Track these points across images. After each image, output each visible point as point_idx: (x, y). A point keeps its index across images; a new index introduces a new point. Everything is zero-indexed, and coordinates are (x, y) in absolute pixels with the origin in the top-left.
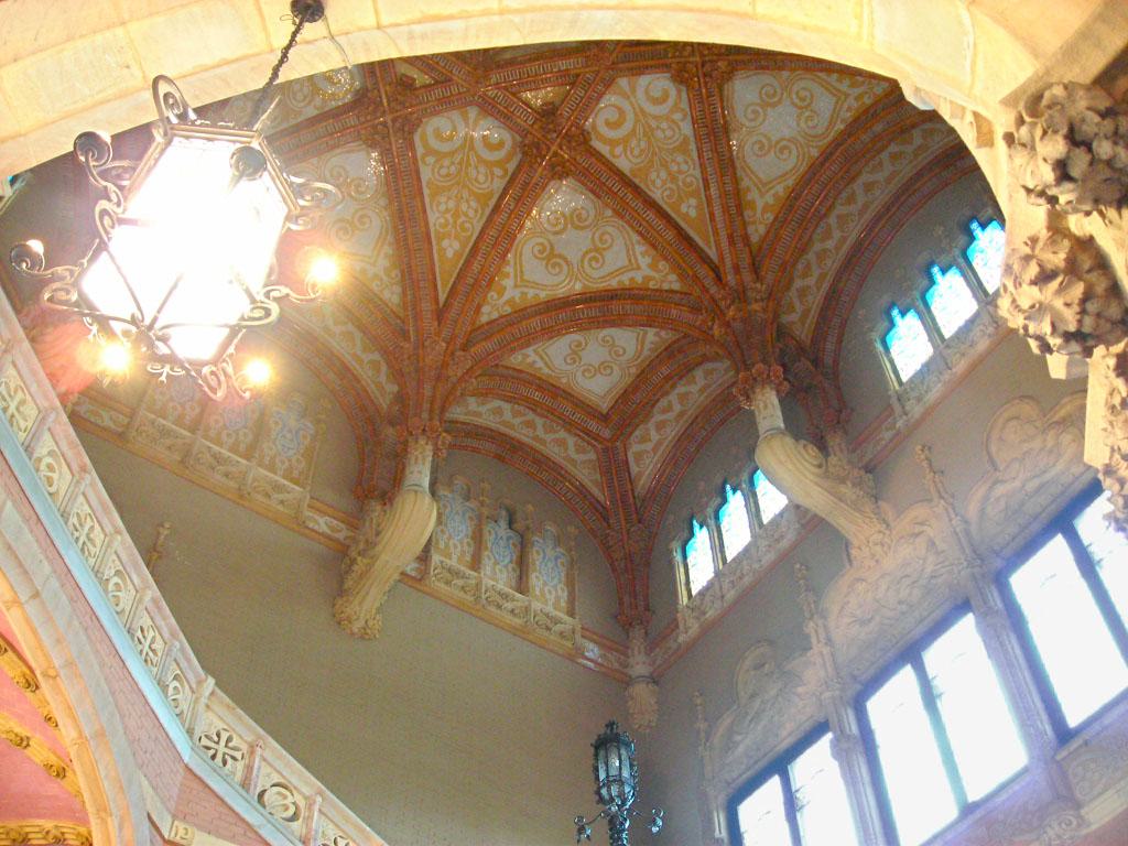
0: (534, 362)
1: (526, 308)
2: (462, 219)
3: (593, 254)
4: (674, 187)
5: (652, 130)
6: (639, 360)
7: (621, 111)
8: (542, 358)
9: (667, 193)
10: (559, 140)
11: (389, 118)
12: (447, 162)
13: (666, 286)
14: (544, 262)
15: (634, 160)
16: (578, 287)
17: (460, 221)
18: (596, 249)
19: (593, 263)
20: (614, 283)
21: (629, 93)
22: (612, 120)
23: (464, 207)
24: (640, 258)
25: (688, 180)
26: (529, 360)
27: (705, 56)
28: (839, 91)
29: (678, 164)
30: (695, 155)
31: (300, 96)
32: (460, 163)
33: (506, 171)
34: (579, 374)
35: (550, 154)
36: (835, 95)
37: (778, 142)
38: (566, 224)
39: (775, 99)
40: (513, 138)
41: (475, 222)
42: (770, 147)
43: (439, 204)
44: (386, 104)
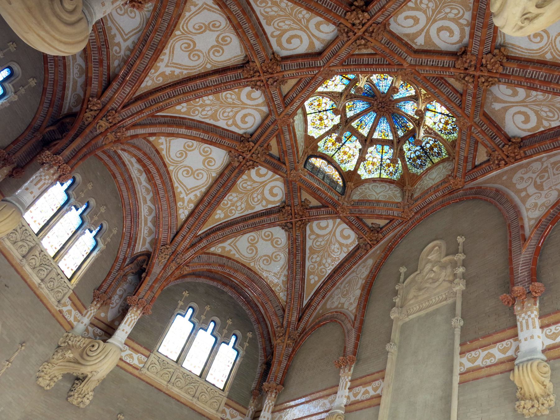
2: (270, 4)
3: (192, 47)
4: (198, 104)
5: (233, 107)
10: (265, 82)
11: (360, 33)
13: (147, 79)
14: (207, 24)
16: (177, 33)
19: (186, 45)
20: (166, 51)
21: (259, 108)
23: (275, 9)
24: (173, 69)
25: (197, 112)
28: (192, 192)
29: (208, 111)
30: (207, 121)
32: (300, 21)
33: (273, 36)
36: (191, 189)
37: (186, 154)
40: (287, 50)
41: (262, 9)
42: (187, 150)
44: (370, 39)
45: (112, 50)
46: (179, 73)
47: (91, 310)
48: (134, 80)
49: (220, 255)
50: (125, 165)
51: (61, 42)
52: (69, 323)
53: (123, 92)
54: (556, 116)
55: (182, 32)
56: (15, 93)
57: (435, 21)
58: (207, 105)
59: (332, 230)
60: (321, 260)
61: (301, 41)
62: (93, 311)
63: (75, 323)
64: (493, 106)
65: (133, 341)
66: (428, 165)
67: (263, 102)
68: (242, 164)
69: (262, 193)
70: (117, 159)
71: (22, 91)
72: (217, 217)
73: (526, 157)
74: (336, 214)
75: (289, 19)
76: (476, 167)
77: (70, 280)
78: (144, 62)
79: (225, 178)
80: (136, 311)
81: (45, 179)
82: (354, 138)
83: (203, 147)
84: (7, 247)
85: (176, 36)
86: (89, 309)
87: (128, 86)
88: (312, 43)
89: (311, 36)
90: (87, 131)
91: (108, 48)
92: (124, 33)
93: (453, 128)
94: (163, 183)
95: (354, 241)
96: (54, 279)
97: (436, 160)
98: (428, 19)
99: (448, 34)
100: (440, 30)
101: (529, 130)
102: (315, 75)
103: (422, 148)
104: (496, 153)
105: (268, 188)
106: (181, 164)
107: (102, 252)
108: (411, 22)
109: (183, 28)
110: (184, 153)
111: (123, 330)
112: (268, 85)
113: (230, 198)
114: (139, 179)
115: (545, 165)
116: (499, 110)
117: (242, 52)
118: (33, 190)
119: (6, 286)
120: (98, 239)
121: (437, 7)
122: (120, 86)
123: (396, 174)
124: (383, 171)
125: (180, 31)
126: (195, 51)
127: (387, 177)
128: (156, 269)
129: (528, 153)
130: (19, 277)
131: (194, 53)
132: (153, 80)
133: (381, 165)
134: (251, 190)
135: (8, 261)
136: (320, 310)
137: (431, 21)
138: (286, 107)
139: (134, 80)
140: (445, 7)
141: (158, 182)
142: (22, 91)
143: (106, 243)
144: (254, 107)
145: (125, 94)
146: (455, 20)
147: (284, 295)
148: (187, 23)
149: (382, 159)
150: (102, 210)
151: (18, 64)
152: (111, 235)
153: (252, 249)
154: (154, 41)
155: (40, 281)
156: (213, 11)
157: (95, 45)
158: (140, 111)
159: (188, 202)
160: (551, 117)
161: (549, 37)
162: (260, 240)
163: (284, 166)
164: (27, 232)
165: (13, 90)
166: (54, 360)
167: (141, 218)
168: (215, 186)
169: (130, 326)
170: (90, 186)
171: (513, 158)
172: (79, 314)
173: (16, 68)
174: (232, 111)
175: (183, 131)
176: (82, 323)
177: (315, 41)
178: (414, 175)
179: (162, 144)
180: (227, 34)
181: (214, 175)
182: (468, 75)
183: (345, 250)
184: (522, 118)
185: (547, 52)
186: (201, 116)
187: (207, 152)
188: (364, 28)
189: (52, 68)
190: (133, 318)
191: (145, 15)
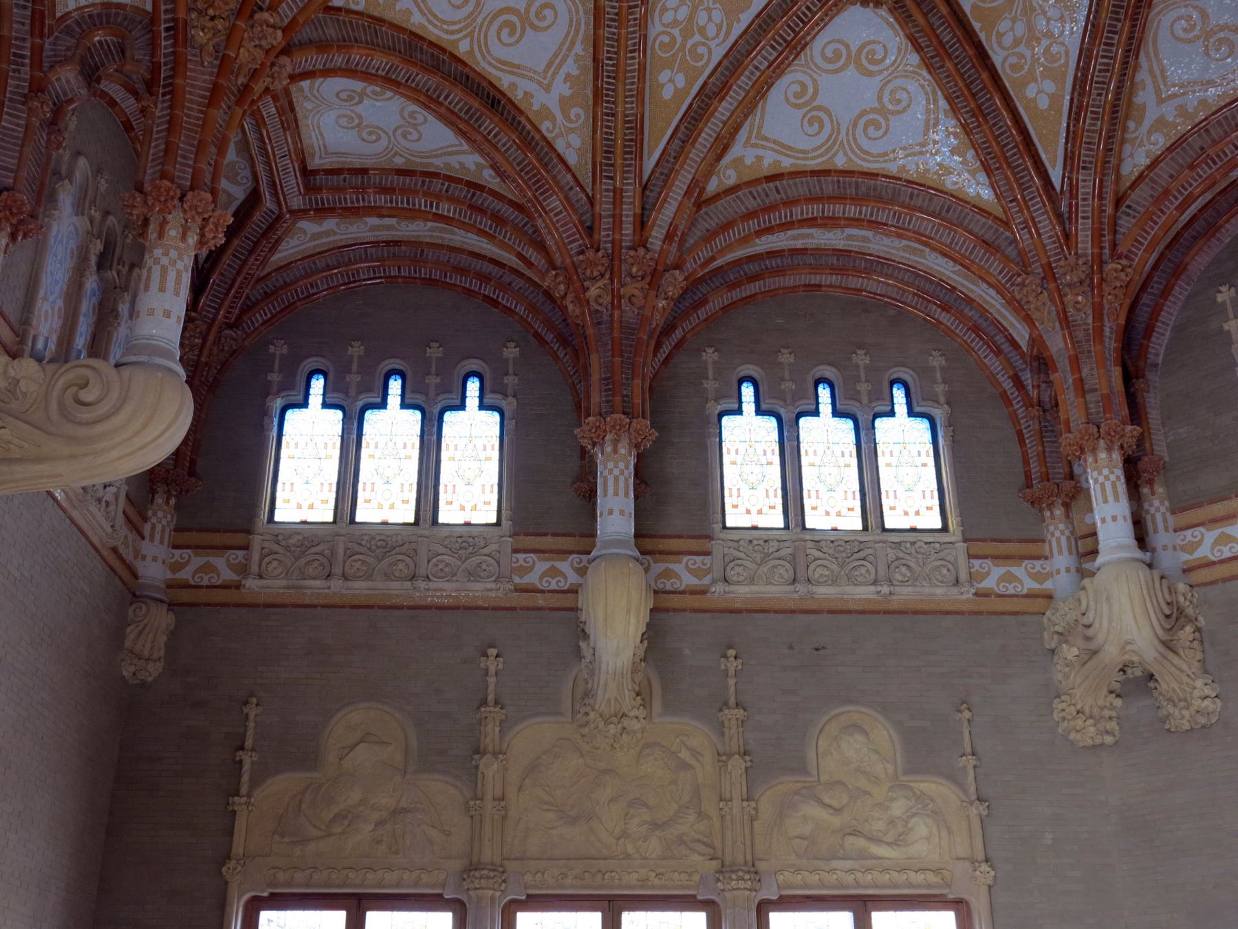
1: (381, 21)
3: (514, 18)
6: (418, 160)
9: (666, 39)
13: (560, 146)
16: (463, 48)
18: (525, 20)
19: (505, 31)
20: (505, 81)
25: (701, 50)
29: (710, 19)
30: (738, 29)
37: (819, 108)
39: (871, 68)
42: (805, 104)
45: (489, 182)
46: (576, 64)
47: (1053, 535)
48: (538, 181)
49: (1170, 149)
50: (804, 251)
51: (138, 433)
52: (1031, 595)
53: (556, 215)
55: (465, 37)
56: (506, 396)
58: (691, 18)
62: (1057, 534)
63: (1048, 585)
65: (1200, 505)
70: (773, 263)
71: (510, 380)
72: (1043, 103)
77: (945, 528)
78: (504, 145)
80: (1096, 461)
81: (611, 471)
83: (819, 60)
84: (749, 596)
85: (471, 52)
86: (1049, 537)
87: (545, 200)
90: (590, 332)
91: (481, 188)
92: (456, 146)
94: (857, 200)
96: (898, 559)
106: (843, 132)
107: (950, 423)
109: (452, 33)
110: (814, 113)
111: (1114, 518)
113: (1008, 40)
114: (850, 237)
118: (609, 507)
119: (817, 649)
120: (917, 409)
122: (541, 215)
125: (460, 39)
126: (527, 10)
128: (1056, 343)
130: (826, 616)
131: (532, 15)
132: (572, 130)
135: (775, 612)
139: (538, 181)
141: (852, 211)
142: (510, 380)
143: (942, 399)
145: (561, 212)
148: (443, 22)
150: (860, 363)
151: (468, 358)
152: (938, 375)
153: (1221, 42)
154: (461, 110)
155: (872, 588)
157: (466, 213)
158: (614, 197)
164: (755, 542)
165: (500, 397)
166: (1064, 683)
167: (955, 281)
169: (1111, 498)
170: (786, 358)
172: (1038, 563)
173: (474, 365)
175: (724, 109)
176: (1058, 572)
179: (759, 159)
186: (718, 41)
187: (837, 55)
189: (508, 300)
190: (1101, 479)
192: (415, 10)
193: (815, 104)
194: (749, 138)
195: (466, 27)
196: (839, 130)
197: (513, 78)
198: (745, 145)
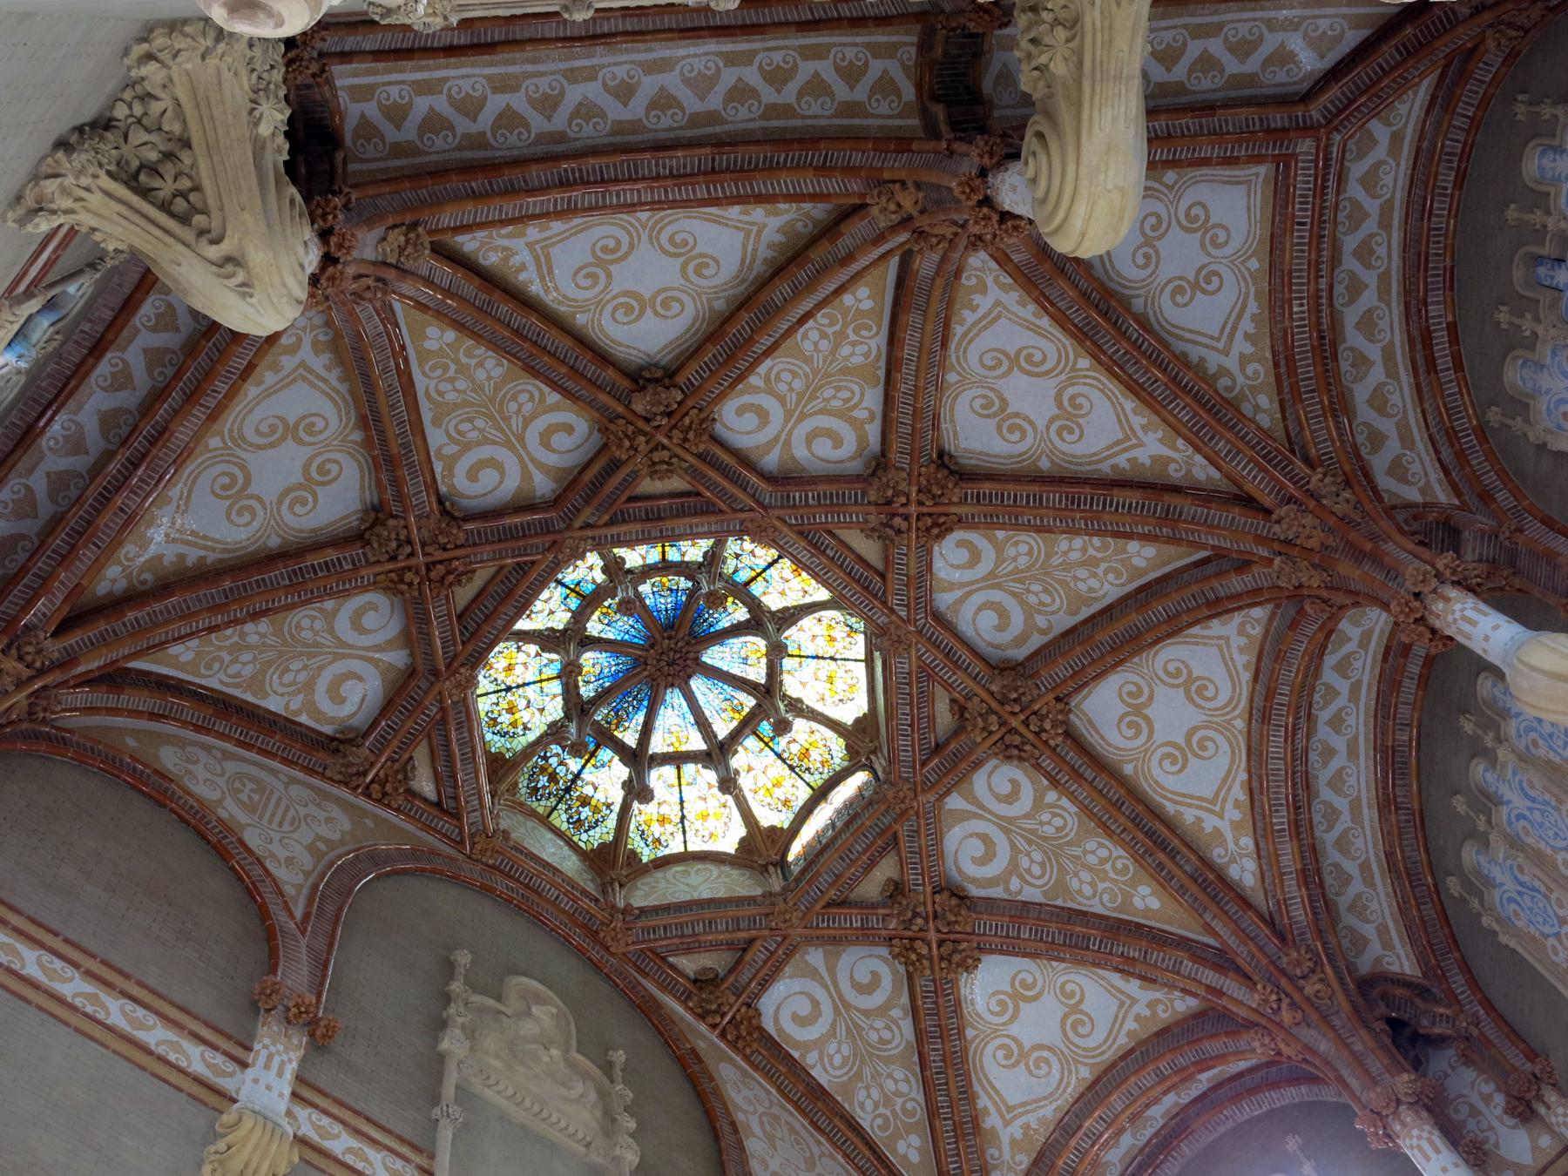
0: (1247, 336)
7: (809, 439)
8: (1234, 329)
9: (863, 333)
10: (901, 510)
12: (1032, 599)
15: (856, 388)
16: (1085, 362)
17: (1099, 555)
20: (1045, 322)
21: (779, 446)
22: (829, 443)
24: (980, 312)
26: (1248, 349)
27: (645, 434)
28: (537, 259)
31: (1058, 822)
32: (1022, 581)
34: (1228, 251)
35: (925, 510)
36: (548, 257)
38: (1010, 417)
39: (623, 300)
42: (693, 258)
43: (1091, 589)
44: (996, 737)
54: (839, 1073)
57: (1006, 831)
58: (836, 346)
59: (351, 647)
60: (250, 648)
61: (958, 567)
64: (812, 949)
66: (541, 807)
67: (793, 457)
68: (641, 424)
69: (486, 441)
73: (746, 1058)
74: (448, 666)
75: (1032, 565)
76: (663, 959)
79: (591, 370)
82: (574, 603)
88: (951, 586)
89: (970, 588)
93: (658, 840)
95: (331, 721)
97: (560, 819)
98: (1010, 820)
99: (978, 854)
100: (985, 839)
101: (780, 1030)
102: (892, 611)
103: (577, 776)
104: (732, 999)
105: (501, 454)
108: (1005, 789)
112: (894, 515)
114: (591, 75)
115: (775, 1110)
116: (806, 962)
117: (965, 450)
121: (1045, 839)
123: (496, 738)
124: (493, 698)
127: (483, 714)
129: (757, 1058)
133: (509, 689)
134: (500, 412)
136: (136, 733)
137: (1006, 825)
138: (801, 533)
140: (1045, 852)
144: (783, 437)
146: (1013, 868)
147: (114, 581)
149: (525, 685)
156: (1111, 447)
159: (505, 249)
160: (831, 1064)
161: (1003, 1024)
162: (309, 451)
163: (606, 518)
167: (439, 68)
168: (569, 343)
171: (738, 1038)
174: (791, 390)
177: (958, 594)
178: (516, 784)
180: (1029, 440)
181: (581, 319)
182: (926, 920)
183: (296, 704)
184: (804, 1008)
185: (975, 1028)
188: (1031, 737)
191: (1138, 296)
192: (1129, 412)
193: (682, 259)
194: (760, 232)
195: (1078, 377)
196: (650, 237)
197: (1037, 321)
198: (765, 226)
